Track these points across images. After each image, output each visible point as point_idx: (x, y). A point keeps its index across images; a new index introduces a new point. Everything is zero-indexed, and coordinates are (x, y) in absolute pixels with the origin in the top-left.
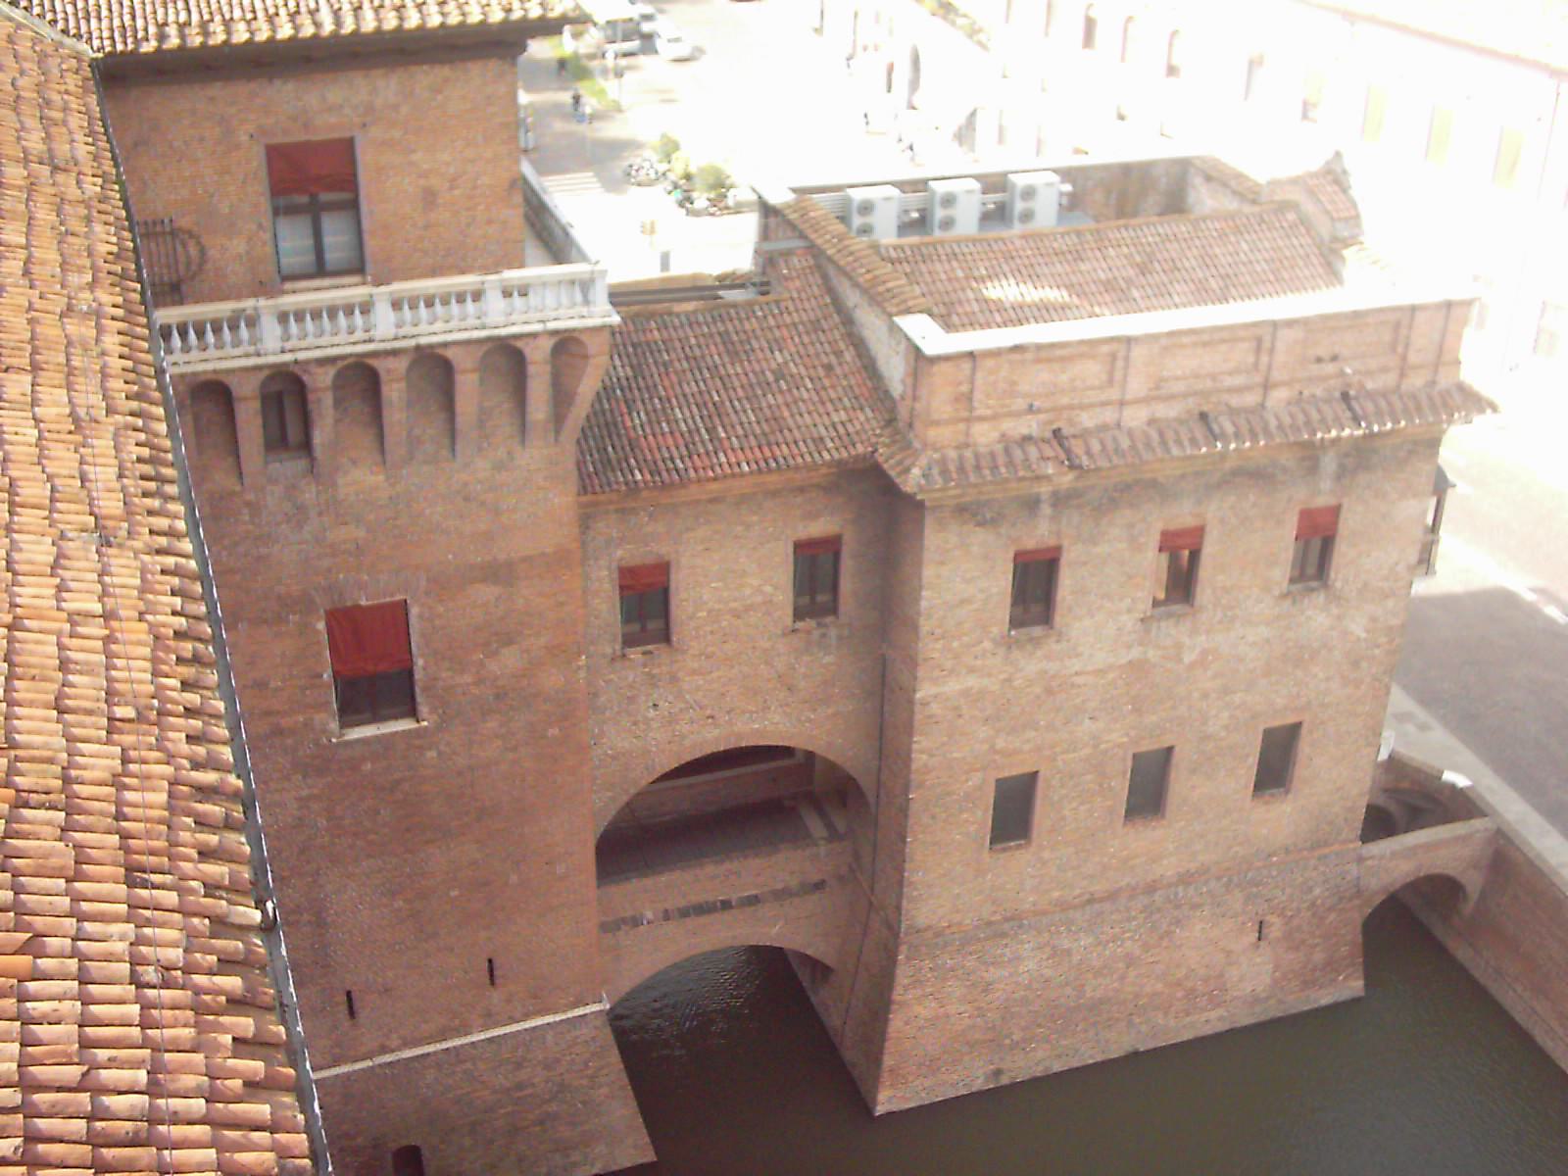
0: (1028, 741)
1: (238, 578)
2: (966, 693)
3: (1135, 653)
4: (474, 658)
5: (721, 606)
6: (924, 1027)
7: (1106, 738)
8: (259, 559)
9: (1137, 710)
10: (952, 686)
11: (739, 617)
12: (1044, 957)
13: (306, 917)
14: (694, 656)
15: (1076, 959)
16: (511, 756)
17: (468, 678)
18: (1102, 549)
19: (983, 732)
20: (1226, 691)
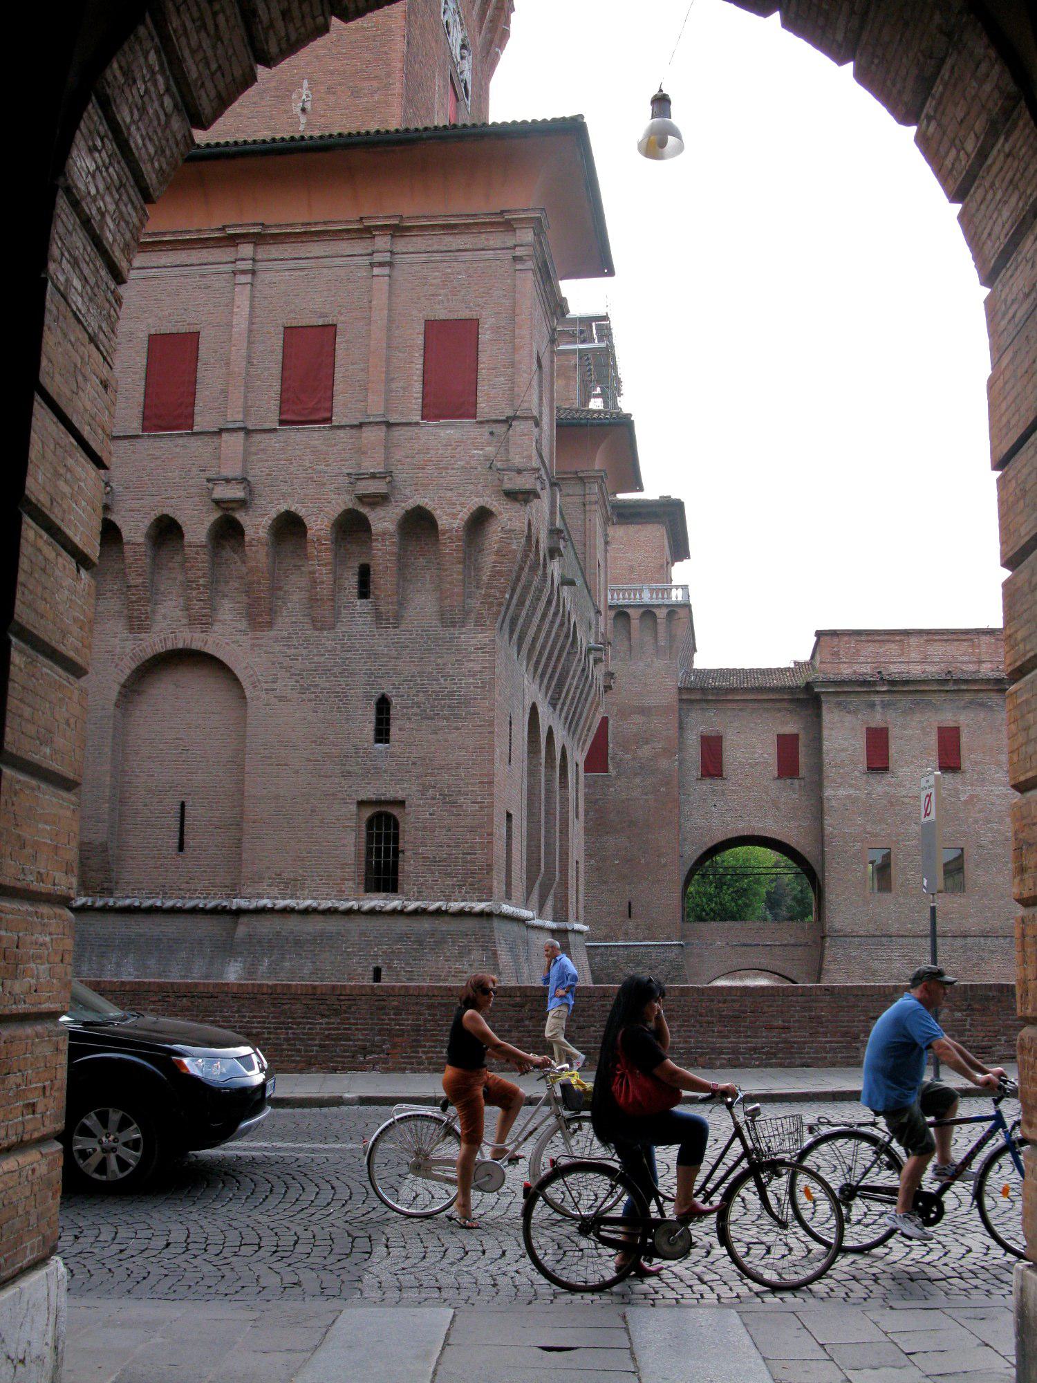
10: (842, 793)
16: (645, 797)
17: (629, 757)
18: (909, 732)
19: (860, 820)
20: (987, 821)
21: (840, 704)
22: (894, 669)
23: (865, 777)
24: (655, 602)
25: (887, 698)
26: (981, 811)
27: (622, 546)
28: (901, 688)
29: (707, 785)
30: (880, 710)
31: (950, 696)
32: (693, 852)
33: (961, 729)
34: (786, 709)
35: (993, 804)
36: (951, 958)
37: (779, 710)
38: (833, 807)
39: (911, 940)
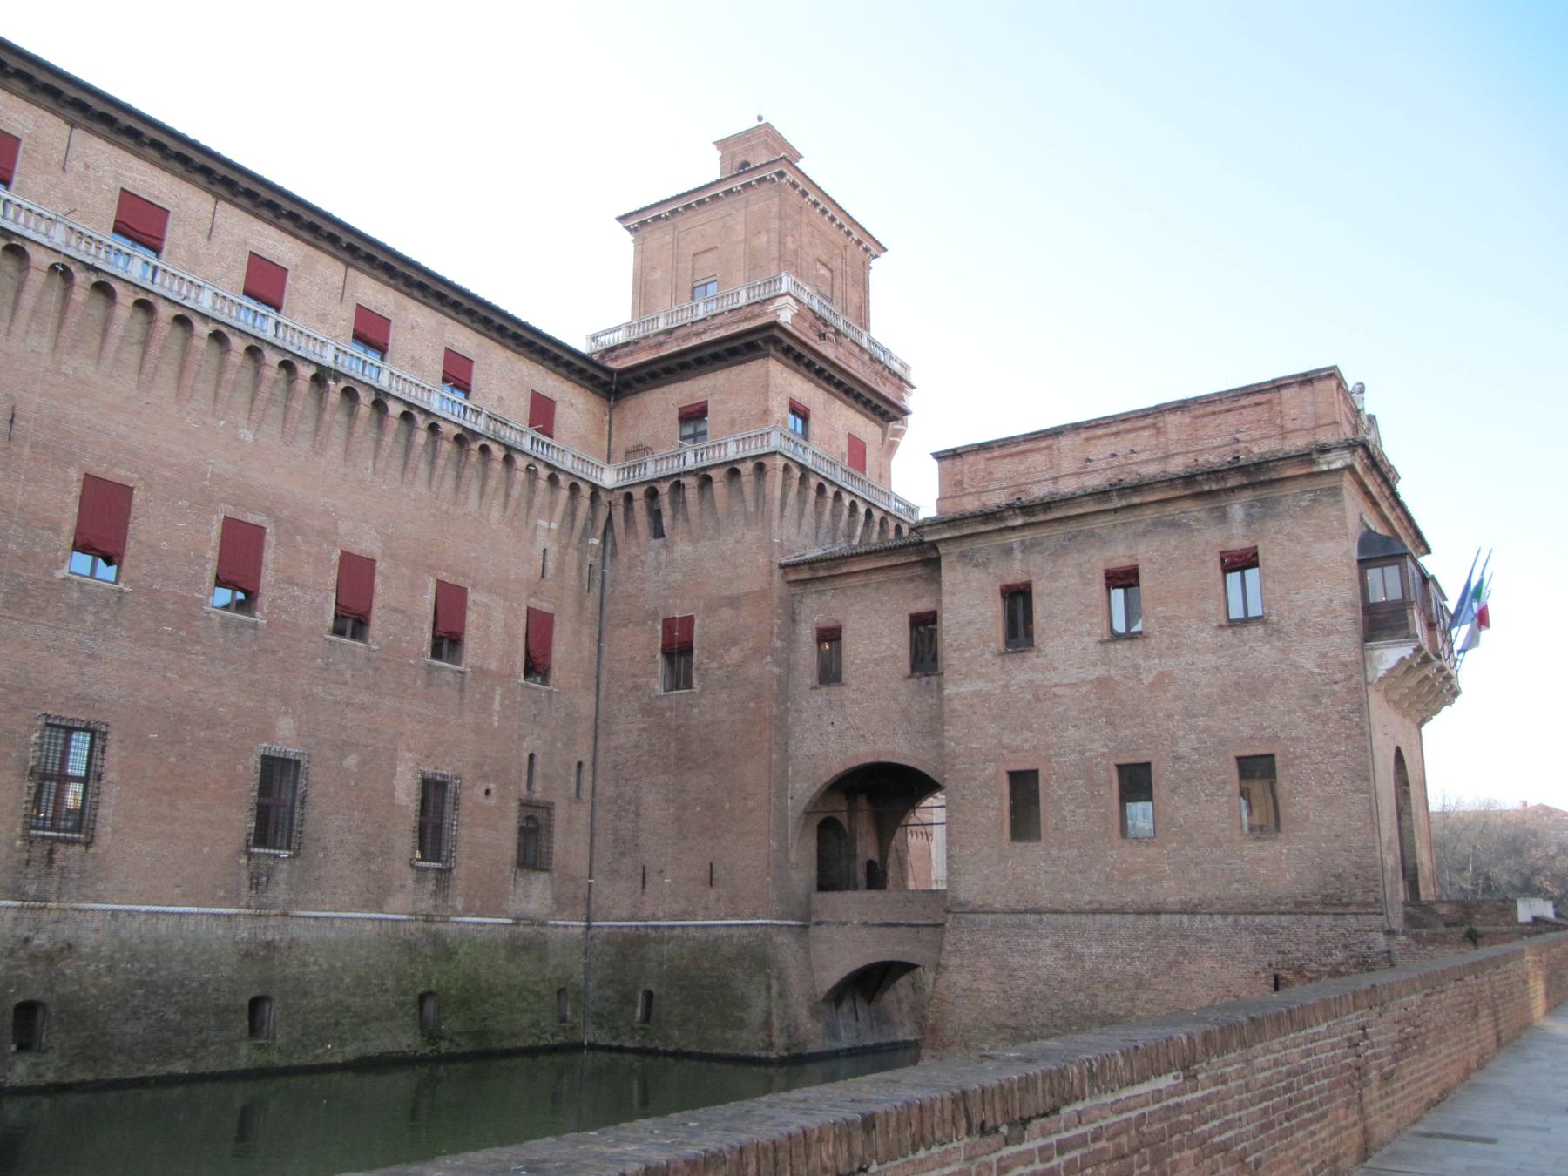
0: (1027, 741)
2: (977, 693)
3: (1100, 671)
4: (719, 652)
5: (868, 657)
6: (961, 997)
7: (1090, 747)
8: (642, 590)
9: (1110, 723)
10: (967, 688)
11: (878, 665)
12: (1060, 956)
14: (854, 690)
15: (1089, 965)
19: (992, 729)
20: (1189, 714)
21: (964, 556)
22: (1039, 492)
23: (999, 661)
25: (1028, 535)
26: (1177, 698)
27: (723, 396)
28: (1041, 517)
29: (821, 697)
31: (1121, 518)
32: (804, 788)
33: (1140, 567)
34: (920, 577)
35: (1196, 685)
36: (1132, 950)
37: (912, 579)
38: (954, 711)
39: (1071, 918)
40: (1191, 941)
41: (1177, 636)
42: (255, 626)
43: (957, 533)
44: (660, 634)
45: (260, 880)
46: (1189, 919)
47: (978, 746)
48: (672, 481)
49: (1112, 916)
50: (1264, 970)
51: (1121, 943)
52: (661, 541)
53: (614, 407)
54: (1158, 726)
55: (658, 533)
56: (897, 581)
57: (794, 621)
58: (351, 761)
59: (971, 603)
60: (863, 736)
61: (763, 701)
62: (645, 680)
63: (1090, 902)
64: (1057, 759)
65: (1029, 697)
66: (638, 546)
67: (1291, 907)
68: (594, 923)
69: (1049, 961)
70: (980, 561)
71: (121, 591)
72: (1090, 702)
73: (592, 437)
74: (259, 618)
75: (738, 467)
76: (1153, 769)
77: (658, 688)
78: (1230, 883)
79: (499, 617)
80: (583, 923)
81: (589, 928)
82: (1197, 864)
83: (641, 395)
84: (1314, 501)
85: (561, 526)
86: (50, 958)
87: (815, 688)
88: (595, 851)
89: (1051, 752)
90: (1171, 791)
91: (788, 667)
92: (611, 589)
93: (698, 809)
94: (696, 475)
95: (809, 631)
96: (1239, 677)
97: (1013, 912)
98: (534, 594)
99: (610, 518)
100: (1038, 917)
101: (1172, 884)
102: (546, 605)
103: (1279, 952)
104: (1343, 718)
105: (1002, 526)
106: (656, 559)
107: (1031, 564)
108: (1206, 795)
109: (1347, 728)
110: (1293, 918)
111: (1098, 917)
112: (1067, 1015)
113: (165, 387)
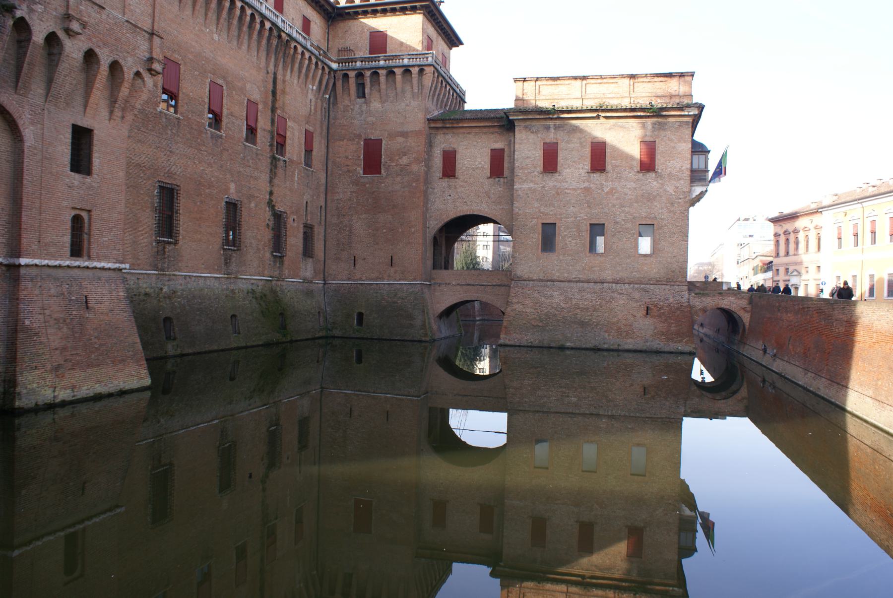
1: (346, 127)
2: (530, 189)
3: (586, 184)
5: (469, 166)
8: (352, 123)
10: (525, 186)
13: (348, 229)
14: (461, 181)
16: (403, 190)
18: (571, 146)
19: (536, 205)
20: (622, 206)
21: (527, 127)
24: (411, 63)
26: (617, 199)
30: (553, 131)
32: (435, 225)
34: (497, 132)
35: (626, 194)
36: (592, 297)
37: (493, 133)
38: (519, 195)
39: (567, 284)
40: (615, 295)
41: (620, 173)
42: (221, 137)
43: (525, 117)
44: (363, 146)
45: (227, 261)
46: (615, 286)
47: (529, 211)
48: (372, 71)
49: (584, 283)
50: (643, 305)
51: (587, 294)
52: (363, 100)
53: (331, 25)
54: (609, 209)
55: (362, 94)
56: (485, 133)
57: (431, 146)
58: (253, 205)
59: (529, 149)
60: (465, 202)
61: (420, 183)
62: (354, 168)
63: (575, 278)
64: (565, 219)
65: (554, 192)
66: (348, 100)
67: (655, 282)
68: (327, 282)
69: (557, 300)
70: (534, 130)
71: (178, 119)
72: (581, 197)
73: (322, 40)
74: (223, 133)
75: (411, 69)
76: (605, 227)
77: (361, 172)
78: (632, 272)
79: (297, 134)
80: (323, 282)
81: (325, 284)
82: (620, 265)
83: (347, 21)
84: (680, 126)
85: (317, 89)
86: (169, 297)
87: (442, 178)
88: (326, 248)
89: (563, 216)
90: (612, 236)
91: (428, 167)
92: (333, 121)
93: (384, 231)
94: (386, 69)
95: (439, 152)
96: (644, 193)
97: (542, 281)
98: (307, 123)
99: (334, 84)
100: (553, 283)
101: (610, 272)
102: (311, 128)
103: (649, 299)
104: (681, 212)
105: (548, 117)
106: (360, 108)
107: (558, 135)
108: (626, 238)
109: (682, 217)
110: (655, 286)
111: (578, 284)
112: (564, 321)
113: (188, 12)
